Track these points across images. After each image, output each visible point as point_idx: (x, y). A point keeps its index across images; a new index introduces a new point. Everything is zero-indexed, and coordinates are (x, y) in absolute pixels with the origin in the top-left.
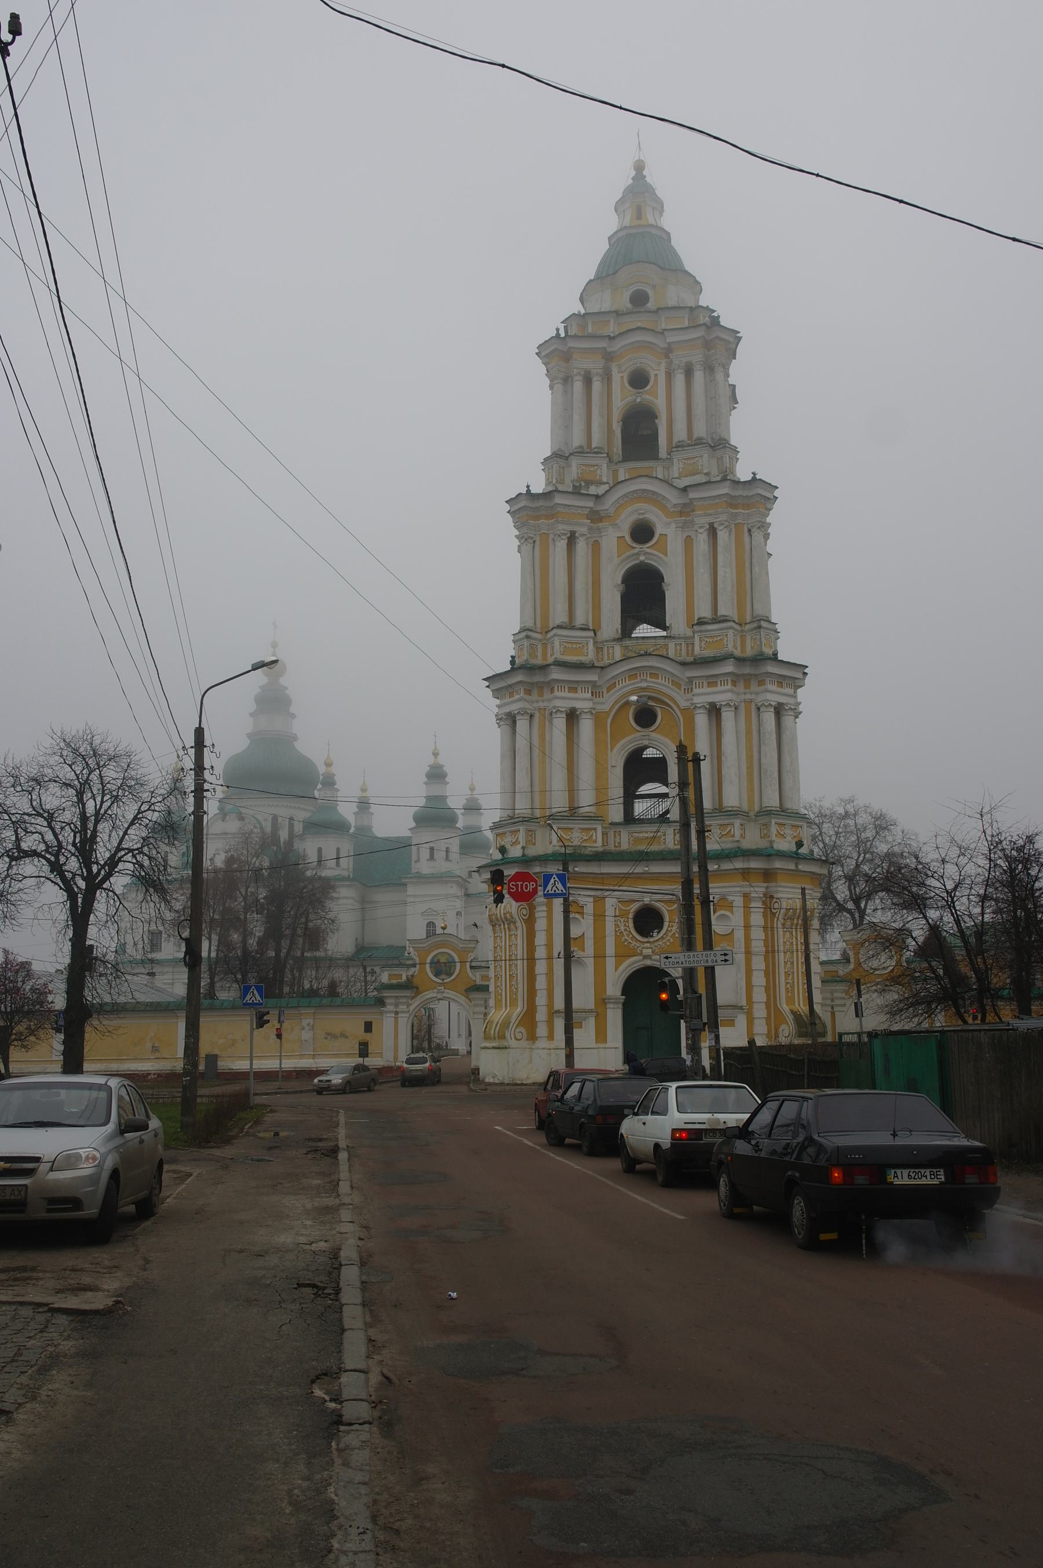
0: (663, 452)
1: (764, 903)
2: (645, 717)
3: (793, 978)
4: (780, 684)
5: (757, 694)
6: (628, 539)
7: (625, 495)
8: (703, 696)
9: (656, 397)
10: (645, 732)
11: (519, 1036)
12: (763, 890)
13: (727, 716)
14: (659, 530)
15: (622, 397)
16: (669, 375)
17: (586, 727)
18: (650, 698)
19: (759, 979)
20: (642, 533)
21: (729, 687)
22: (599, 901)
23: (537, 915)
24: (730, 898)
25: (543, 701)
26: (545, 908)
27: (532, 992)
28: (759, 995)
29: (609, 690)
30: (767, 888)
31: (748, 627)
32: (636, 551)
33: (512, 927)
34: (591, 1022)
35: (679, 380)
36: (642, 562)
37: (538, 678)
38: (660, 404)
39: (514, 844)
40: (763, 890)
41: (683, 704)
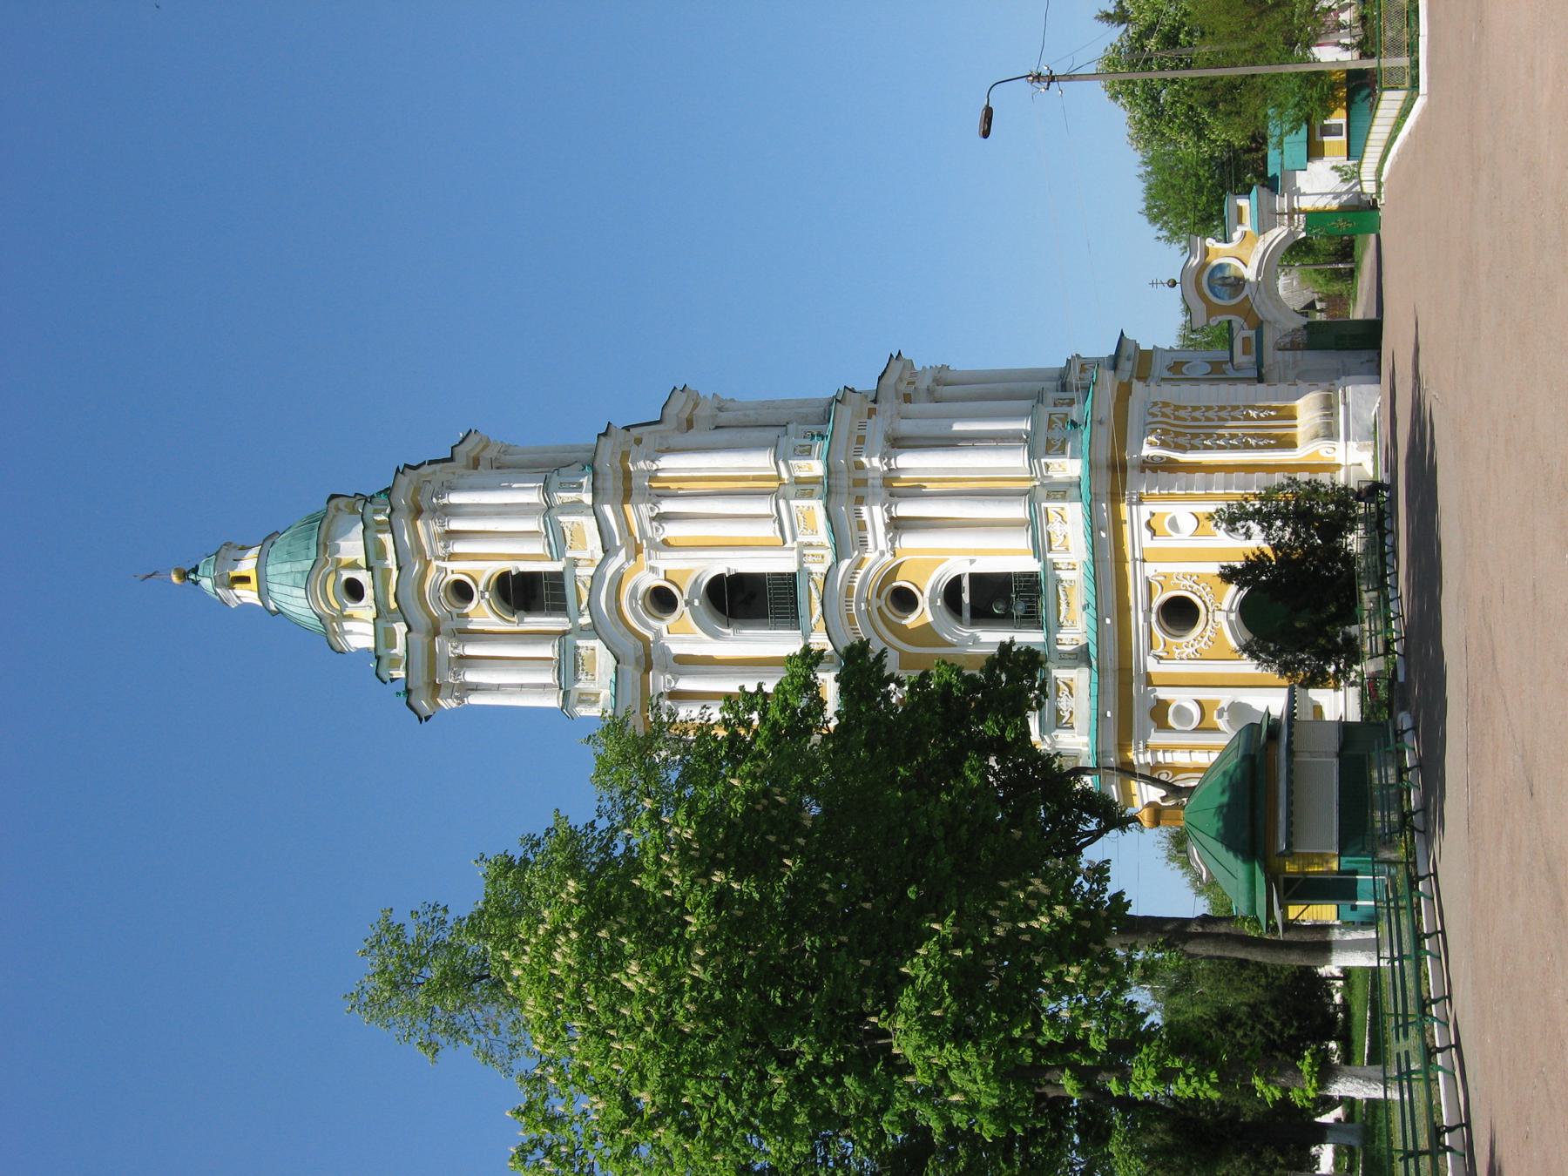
0: (557, 567)
2: (905, 600)
4: (861, 440)
6: (671, 619)
8: (878, 535)
9: (484, 572)
10: (923, 602)
13: (905, 509)
14: (657, 581)
15: (483, 614)
18: (879, 596)
20: (662, 600)
21: (864, 510)
24: (1145, 517)
31: (785, 475)
32: (687, 610)
35: (458, 547)
41: (888, 557)
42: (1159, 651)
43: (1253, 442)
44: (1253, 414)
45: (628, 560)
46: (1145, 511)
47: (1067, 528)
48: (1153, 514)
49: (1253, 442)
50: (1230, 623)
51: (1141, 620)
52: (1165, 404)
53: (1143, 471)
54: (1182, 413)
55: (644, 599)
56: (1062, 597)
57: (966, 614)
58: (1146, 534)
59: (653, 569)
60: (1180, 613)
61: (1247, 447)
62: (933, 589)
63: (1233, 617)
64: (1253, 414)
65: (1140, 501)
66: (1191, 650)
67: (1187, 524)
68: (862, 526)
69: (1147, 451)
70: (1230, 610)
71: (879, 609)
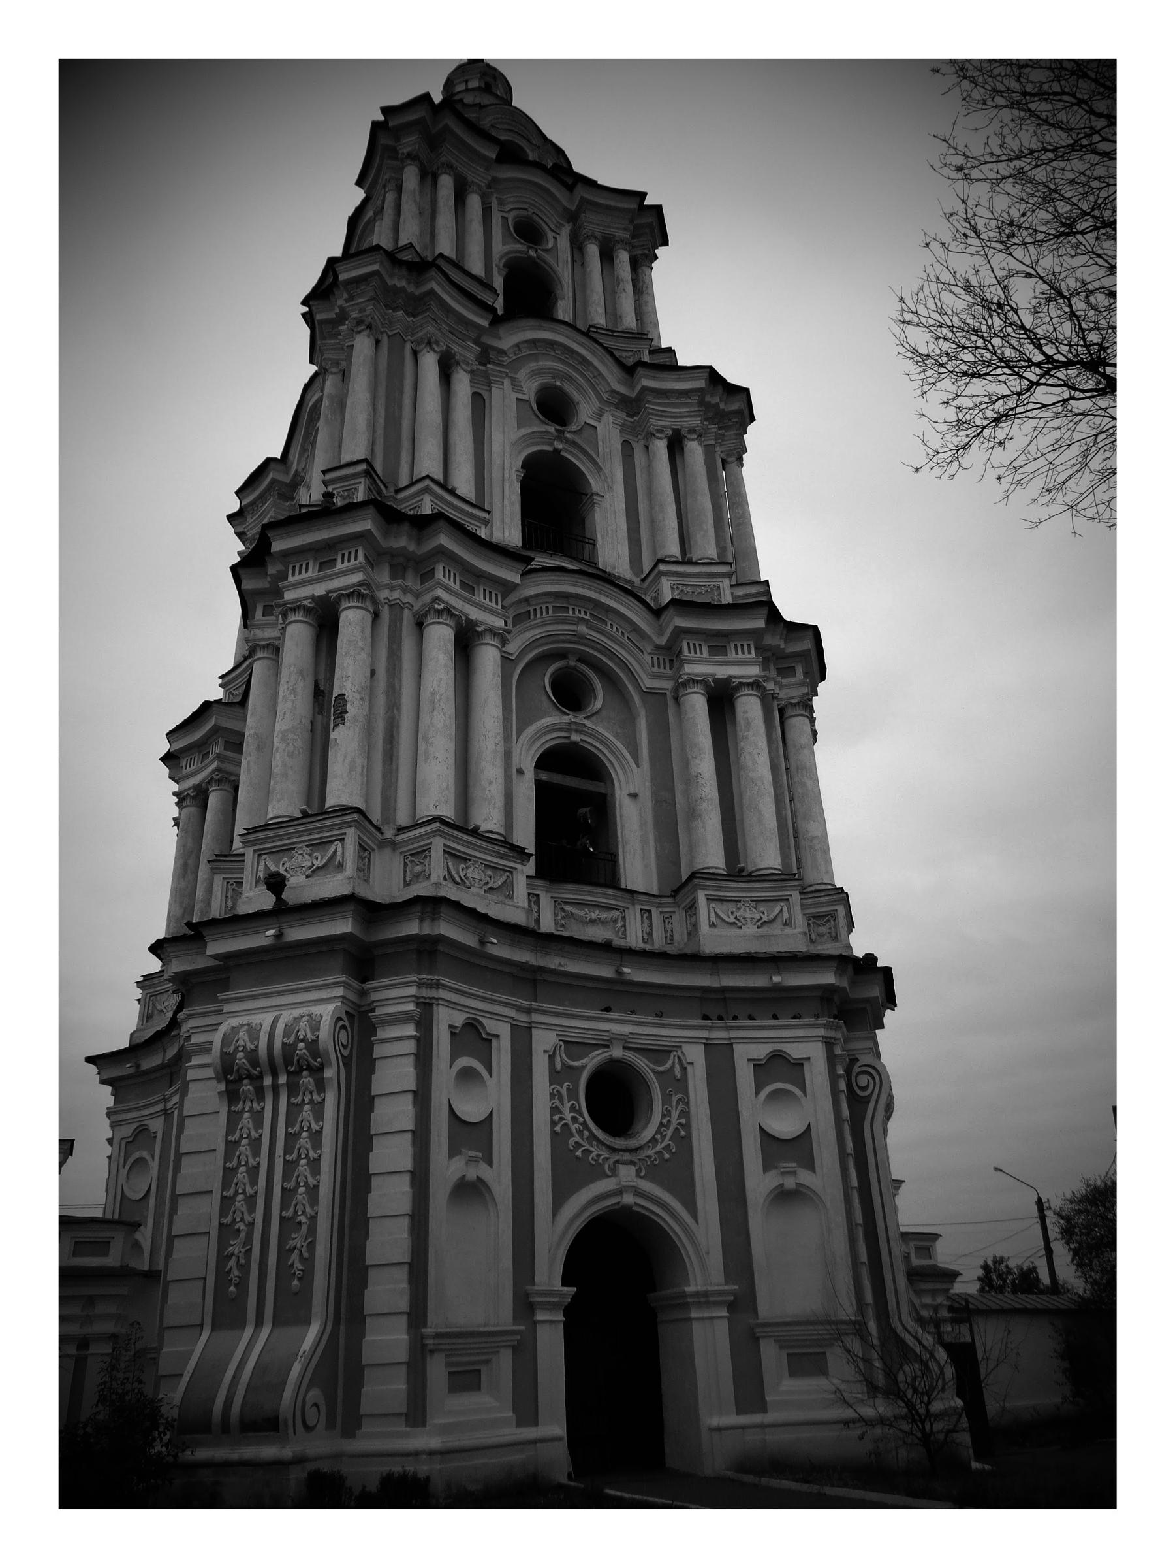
2: (570, 694)
5: (781, 687)
7: (534, 343)
8: (701, 666)
16: (577, 246)
17: (488, 658)
18: (583, 659)
23: (378, 1051)
24: (795, 1051)
25: (405, 590)
26: (410, 1030)
27: (353, 1270)
29: (519, 619)
33: (306, 1080)
34: (504, 1361)
36: (556, 451)
37: (402, 541)
38: (564, 271)
39: (314, 872)
41: (648, 683)
45: (613, 391)
47: (750, 929)
48: (799, 1064)
50: (619, 1192)
51: (622, 1030)
55: (556, 387)
56: (604, 915)
57: (544, 776)
58: (761, 1052)
59: (599, 415)
60: (614, 1098)
62: (594, 735)
63: (628, 1199)
65: (829, 1044)
66: (568, 1115)
67: (785, 1125)
68: (722, 650)
71: (562, 655)
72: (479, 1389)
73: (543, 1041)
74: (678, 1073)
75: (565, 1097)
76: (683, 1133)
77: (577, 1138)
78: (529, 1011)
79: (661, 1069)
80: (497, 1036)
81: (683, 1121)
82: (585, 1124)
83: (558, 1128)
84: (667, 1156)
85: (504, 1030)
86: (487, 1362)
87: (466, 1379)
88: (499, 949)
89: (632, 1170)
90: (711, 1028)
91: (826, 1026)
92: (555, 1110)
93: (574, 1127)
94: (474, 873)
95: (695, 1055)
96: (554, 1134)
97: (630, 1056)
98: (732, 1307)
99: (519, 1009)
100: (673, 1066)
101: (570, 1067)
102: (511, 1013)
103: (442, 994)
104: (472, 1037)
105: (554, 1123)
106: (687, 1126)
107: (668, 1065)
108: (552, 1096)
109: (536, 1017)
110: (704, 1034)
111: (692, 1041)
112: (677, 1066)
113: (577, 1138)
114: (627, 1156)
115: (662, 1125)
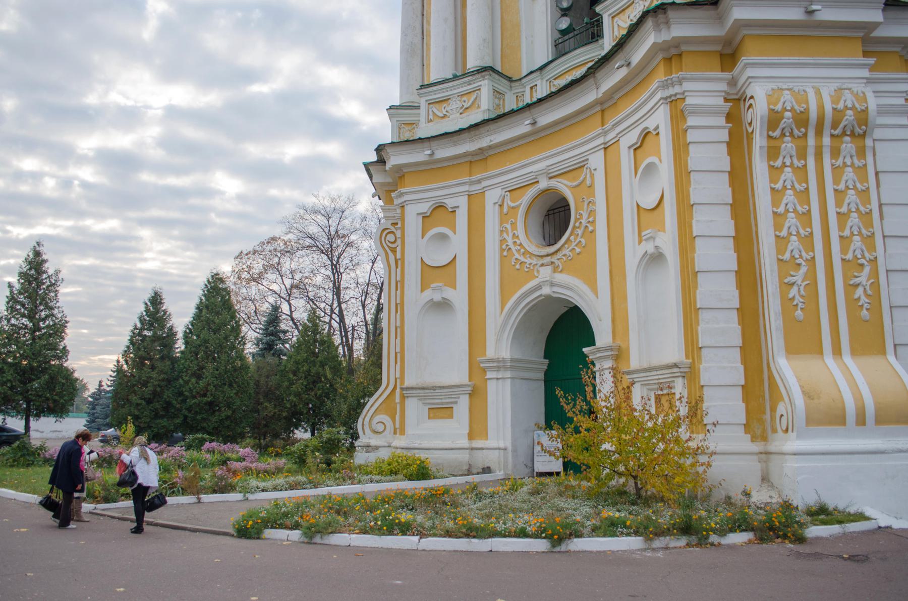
1: (729, 117)
3: (812, 274)
11: (380, 428)
12: (723, 86)
19: (719, 289)
22: (475, 200)
28: (721, 329)
30: (733, 82)
40: (723, 86)
42: (508, 202)
43: (798, 277)
44: (863, 278)
46: (660, 119)
49: (798, 277)
50: (538, 287)
51: (539, 168)
52: (863, 117)
53: (726, 100)
54: (848, 146)
58: (633, 137)
60: (555, 217)
61: (785, 266)
63: (546, 290)
64: (863, 278)
69: (759, 93)
70: (552, 284)
72: (451, 417)
73: (492, 196)
74: (588, 182)
75: (510, 230)
76: (591, 228)
77: (517, 256)
78: (479, 181)
79: (575, 184)
80: (458, 207)
81: (591, 219)
82: (521, 245)
83: (505, 253)
84: (578, 250)
85: (462, 202)
86: (456, 403)
87: (441, 411)
88: (445, 151)
89: (549, 269)
90: (605, 133)
91: (664, 86)
92: (503, 241)
93: (513, 248)
94: (455, 104)
95: (597, 161)
96: (502, 257)
97: (553, 183)
98: (617, 358)
99: (472, 183)
100: (585, 178)
101: (513, 208)
102: (466, 188)
103: (405, 198)
104: (439, 213)
105: (502, 250)
106: (593, 222)
107: (581, 179)
108: (501, 231)
109: (484, 184)
110: (601, 140)
111: (594, 150)
112: (588, 176)
113: (517, 256)
114: (548, 259)
115: (574, 227)
